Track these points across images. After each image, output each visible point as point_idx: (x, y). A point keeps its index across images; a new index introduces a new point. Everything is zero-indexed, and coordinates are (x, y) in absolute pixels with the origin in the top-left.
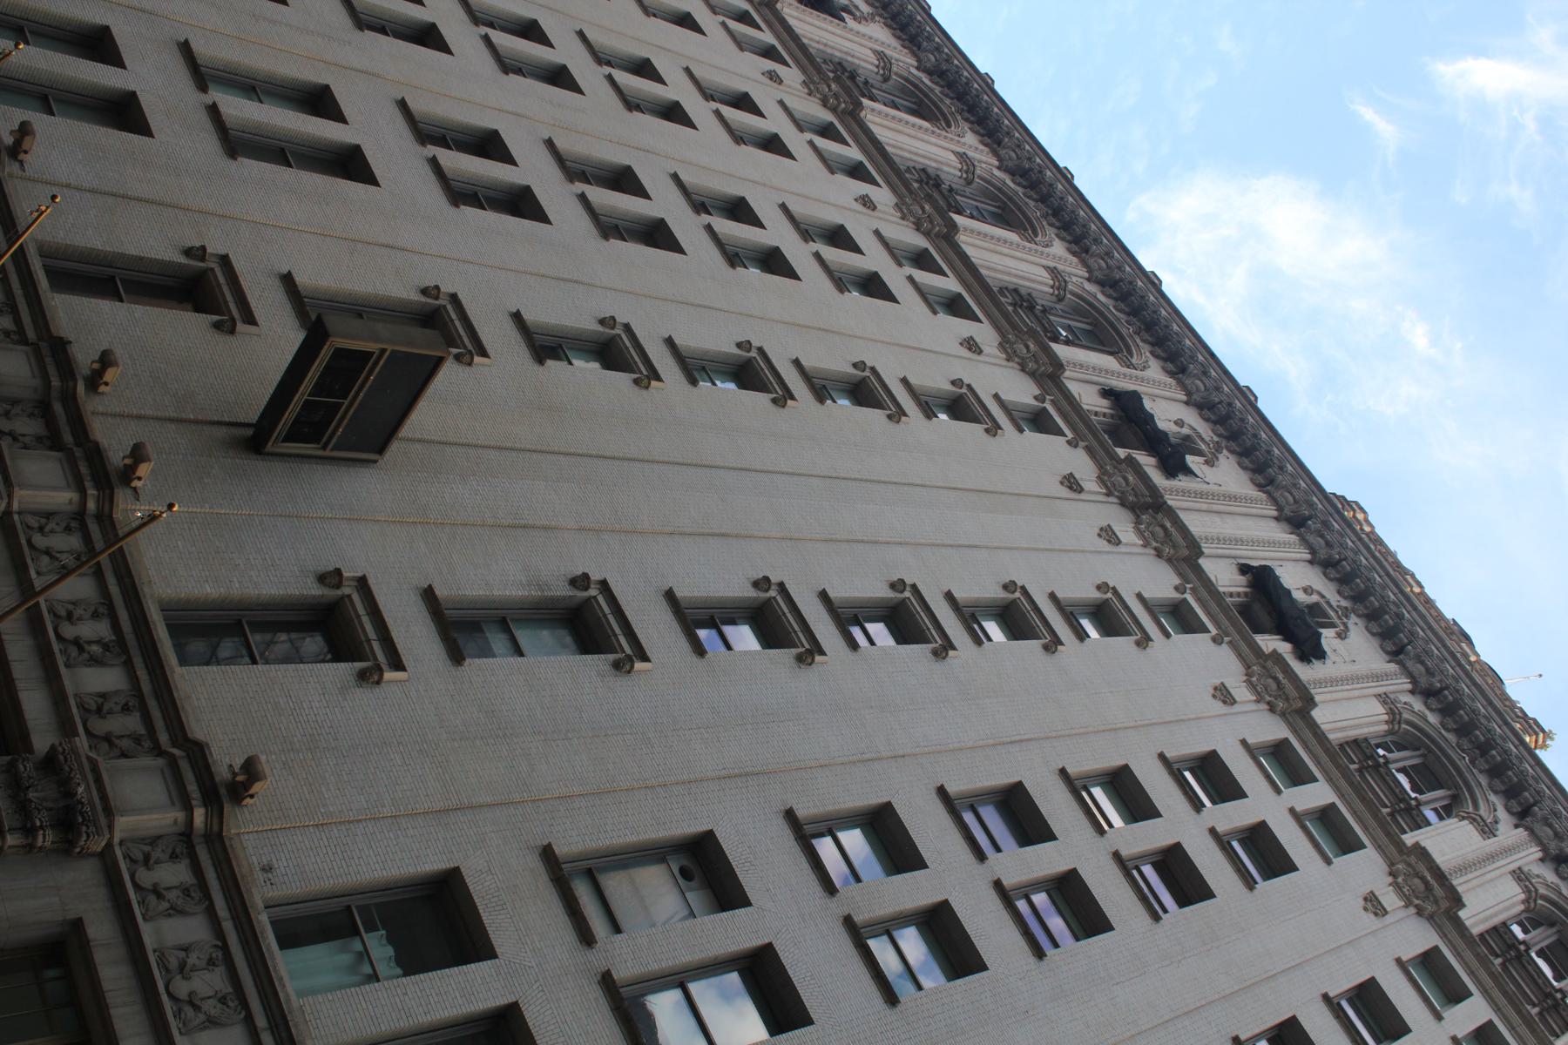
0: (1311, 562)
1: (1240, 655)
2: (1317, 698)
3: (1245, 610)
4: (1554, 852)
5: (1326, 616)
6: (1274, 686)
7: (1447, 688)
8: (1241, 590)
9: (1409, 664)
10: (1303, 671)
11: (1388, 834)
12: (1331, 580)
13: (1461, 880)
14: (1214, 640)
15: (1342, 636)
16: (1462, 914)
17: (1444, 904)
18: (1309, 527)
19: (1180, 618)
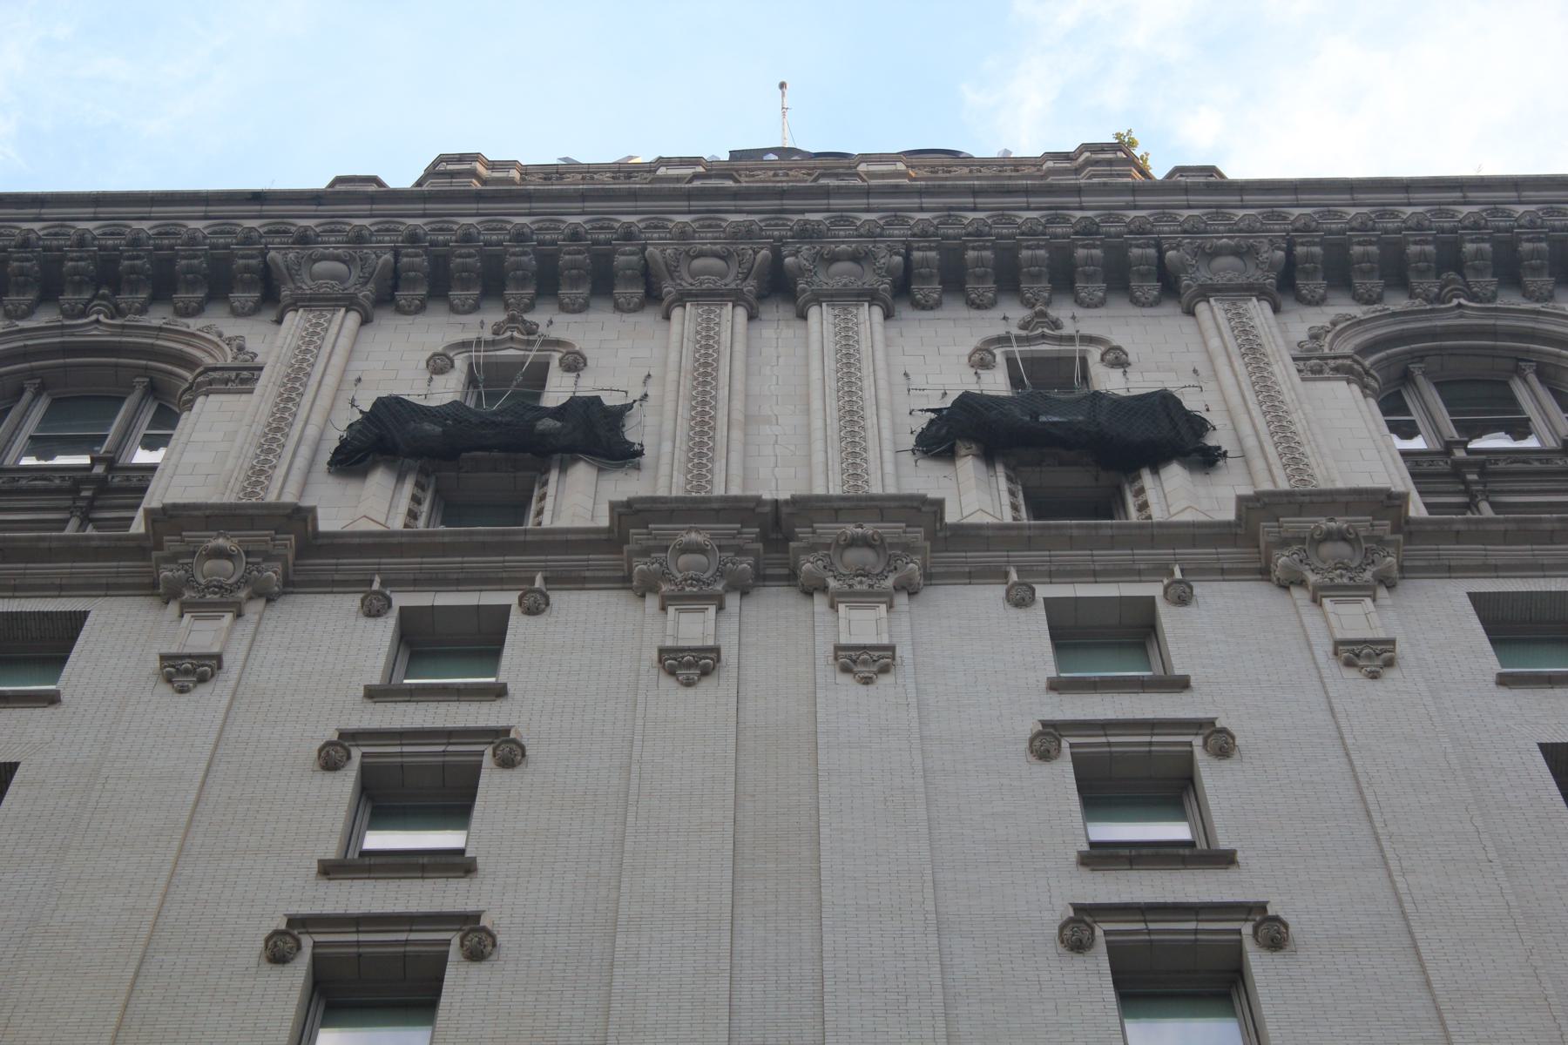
0: (365, 321)
1: (1224, 573)
2: (289, 497)
3: (450, 508)
4: (885, 286)
5: (516, 365)
6: (866, 556)
7: (909, 250)
8: (408, 488)
9: (1204, 276)
10: (662, 475)
11: (1113, 542)
12: (420, 309)
13: (719, 479)
14: (532, 611)
15: (575, 363)
16: (951, 517)
17: (917, 535)
18: (801, 271)
19: (452, 645)
